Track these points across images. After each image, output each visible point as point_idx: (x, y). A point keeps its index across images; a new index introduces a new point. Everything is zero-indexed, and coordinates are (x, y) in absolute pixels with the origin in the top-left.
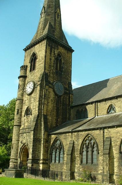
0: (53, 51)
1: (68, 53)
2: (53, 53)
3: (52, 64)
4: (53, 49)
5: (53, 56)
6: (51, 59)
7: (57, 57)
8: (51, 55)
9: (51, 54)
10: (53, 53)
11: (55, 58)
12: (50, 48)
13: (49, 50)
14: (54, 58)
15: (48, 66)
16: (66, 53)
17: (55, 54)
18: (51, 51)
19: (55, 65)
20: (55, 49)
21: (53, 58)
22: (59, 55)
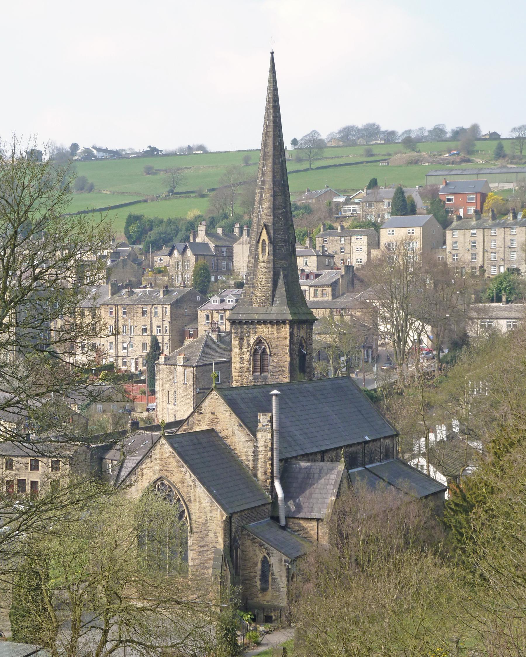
0: (245, 342)
1: (279, 330)
2: (245, 346)
3: (246, 367)
4: (245, 338)
5: (246, 350)
6: (241, 359)
7: (256, 350)
8: (241, 352)
9: (241, 349)
10: (245, 346)
11: (251, 355)
12: (238, 338)
13: (237, 342)
14: (248, 353)
15: (237, 374)
16: (275, 333)
17: (248, 344)
18: (241, 343)
19: (251, 366)
20: (249, 335)
21: (247, 356)
22: (259, 342)
